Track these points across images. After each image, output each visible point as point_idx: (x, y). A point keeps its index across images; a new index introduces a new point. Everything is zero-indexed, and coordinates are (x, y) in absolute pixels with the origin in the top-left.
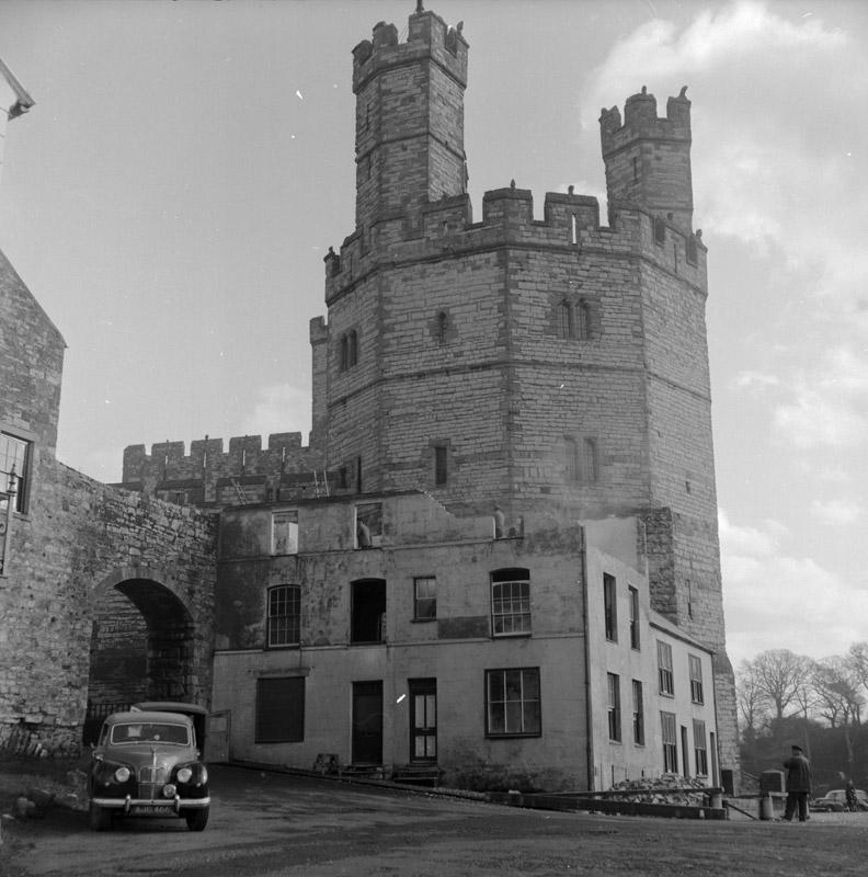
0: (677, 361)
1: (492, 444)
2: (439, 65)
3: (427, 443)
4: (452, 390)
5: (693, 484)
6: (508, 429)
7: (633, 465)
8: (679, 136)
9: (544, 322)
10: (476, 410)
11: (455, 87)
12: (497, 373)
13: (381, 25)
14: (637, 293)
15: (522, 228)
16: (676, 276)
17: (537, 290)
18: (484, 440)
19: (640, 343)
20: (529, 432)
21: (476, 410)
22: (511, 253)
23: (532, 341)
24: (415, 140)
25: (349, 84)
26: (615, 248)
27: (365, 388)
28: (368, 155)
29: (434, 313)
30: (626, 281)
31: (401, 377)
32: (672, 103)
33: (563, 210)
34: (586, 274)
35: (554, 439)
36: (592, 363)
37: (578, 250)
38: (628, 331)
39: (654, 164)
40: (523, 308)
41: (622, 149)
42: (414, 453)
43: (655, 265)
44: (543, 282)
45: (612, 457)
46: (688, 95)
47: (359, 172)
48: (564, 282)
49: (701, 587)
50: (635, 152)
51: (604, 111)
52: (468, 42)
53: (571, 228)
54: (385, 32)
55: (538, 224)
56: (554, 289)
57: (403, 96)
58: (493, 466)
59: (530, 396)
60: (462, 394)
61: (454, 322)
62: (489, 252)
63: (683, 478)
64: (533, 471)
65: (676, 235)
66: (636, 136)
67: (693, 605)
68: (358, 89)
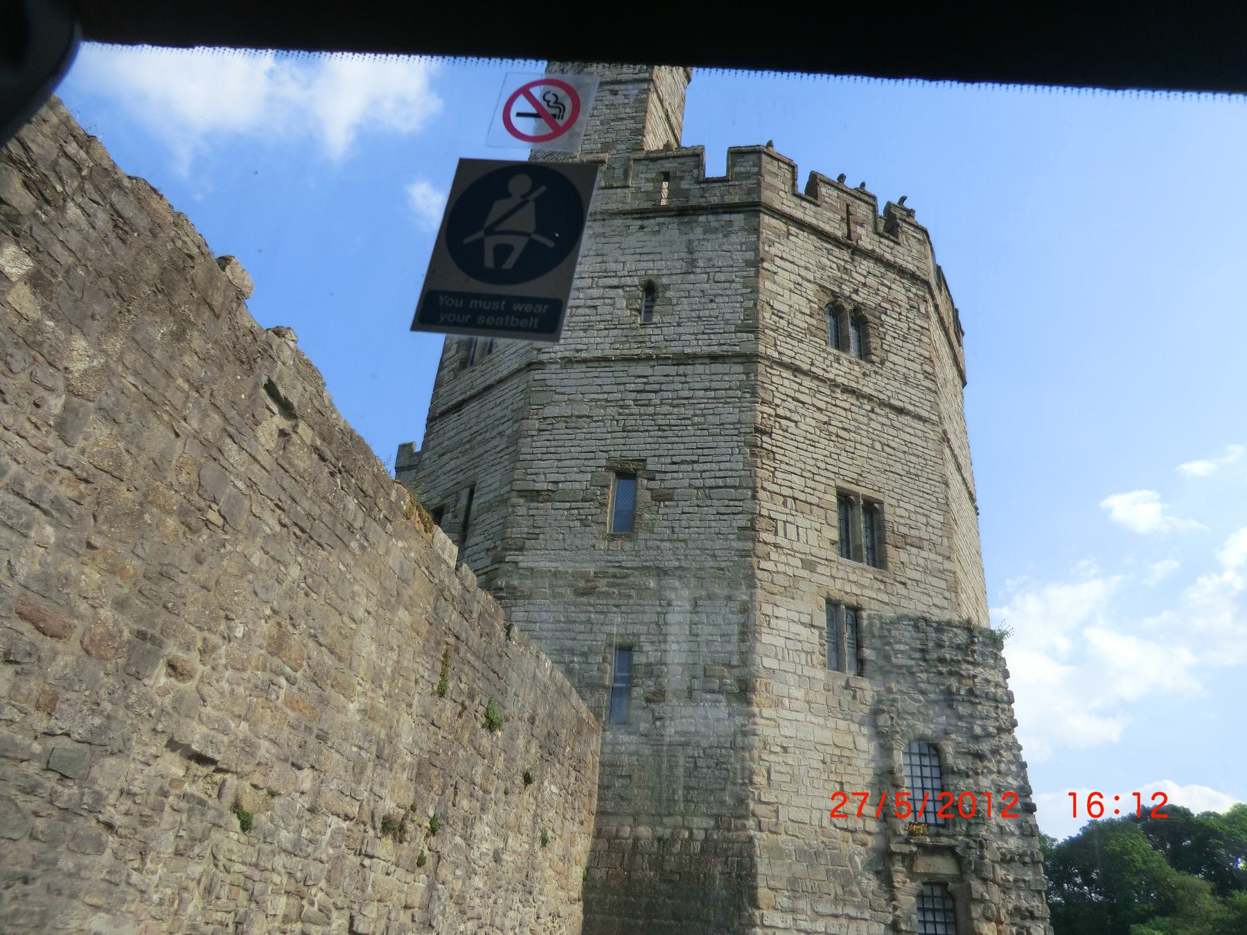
1: (722, 474)
3: (604, 463)
4: (656, 387)
9: (808, 319)
10: (696, 419)
12: (739, 368)
15: (782, 194)
18: (706, 467)
20: (784, 466)
21: (696, 419)
23: (793, 338)
27: (501, 381)
30: (912, 307)
42: (579, 477)
44: (806, 268)
45: (904, 536)
56: (822, 282)
58: (723, 510)
59: (788, 414)
62: (731, 213)
64: (791, 530)
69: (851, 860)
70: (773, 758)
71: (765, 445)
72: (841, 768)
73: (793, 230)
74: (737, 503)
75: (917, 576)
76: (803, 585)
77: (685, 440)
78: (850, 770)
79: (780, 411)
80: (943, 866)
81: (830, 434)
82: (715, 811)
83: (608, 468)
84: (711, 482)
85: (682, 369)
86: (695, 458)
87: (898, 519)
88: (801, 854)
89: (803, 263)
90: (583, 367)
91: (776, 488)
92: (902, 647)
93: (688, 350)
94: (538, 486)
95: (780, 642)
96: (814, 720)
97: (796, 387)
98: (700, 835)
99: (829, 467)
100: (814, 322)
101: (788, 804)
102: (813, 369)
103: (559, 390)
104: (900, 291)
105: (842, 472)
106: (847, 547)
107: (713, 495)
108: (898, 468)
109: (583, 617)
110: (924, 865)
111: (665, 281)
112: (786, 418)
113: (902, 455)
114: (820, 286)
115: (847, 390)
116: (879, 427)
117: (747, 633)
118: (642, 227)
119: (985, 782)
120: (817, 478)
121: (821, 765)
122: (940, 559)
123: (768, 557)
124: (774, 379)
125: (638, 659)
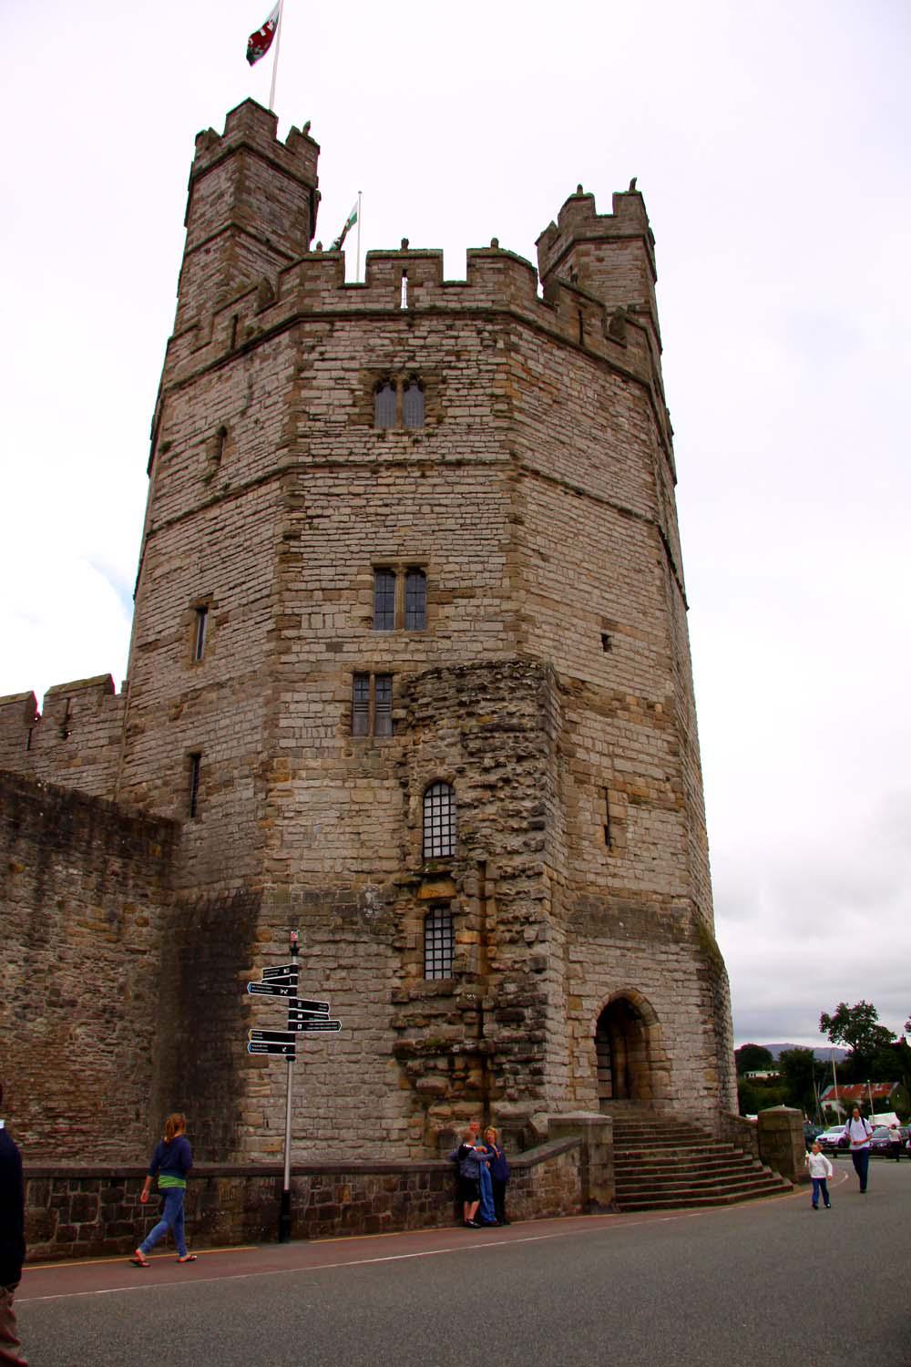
0: (586, 462)
3: (187, 605)
5: (616, 638)
6: (282, 561)
7: (486, 601)
8: (628, 229)
9: (348, 410)
12: (276, 485)
13: (198, 136)
14: (504, 360)
15: (324, 294)
16: (579, 348)
17: (343, 369)
18: (249, 585)
19: (505, 424)
20: (311, 563)
22: (308, 327)
24: (219, 239)
26: (467, 304)
29: (213, 431)
31: (170, 524)
33: (389, 266)
34: (421, 342)
35: (354, 570)
36: (423, 457)
37: (413, 316)
38: (486, 411)
39: (594, 265)
40: (317, 393)
42: (173, 623)
43: (538, 330)
44: (353, 358)
46: (638, 188)
48: (386, 355)
49: (636, 800)
50: (571, 260)
52: (318, 141)
53: (398, 288)
57: (210, 199)
58: (259, 619)
59: (319, 512)
60: (233, 527)
61: (233, 435)
62: (280, 334)
63: (597, 628)
65: (582, 300)
66: (571, 239)
67: (614, 830)
69: (363, 896)
70: (286, 822)
71: (293, 550)
72: (357, 820)
73: (338, 325)
74: (268, 610)
75: (466, 625)
76: (327, 668)
77: (238, 565)
78: (369, 821)
79: (310, 512)
80: (442, 889)
81: (368, 515)
82: (243, 873)
83: (190, 608)
84: (252, 598)
85: (239, 502)
86: (242, 580)
87: (443, 576)
88: (311, 896)
89: (347, 355)
90: (178, 526)
91: (303, 586)
92: (425, 700)
93: (243, 482)
94: (150, 639)
95: (300, 723)
96: (332, 784)
97: (330, 482)
98: (233, 892)
99: (363, 548)
100: (357, 410)
101: (301, 858)
102: (351, 458)
103: (164, 551)
104: (468, 337)
105: (379, 548)
106: (381, 616)
107: (253, 609)
108: (450, 523)
109: (172, 738)
110: (427, 891)
111: (233, 422)
112: (318, 516)
113: (457, 510)
114: (369, 369)
115: (391, 465)
116: (429, 489)
117: (271, 723)
118: (220, 377)
119: (491, 810)
120: (348, 563)
121: (335, 821)
122: (497, 602)
123: (287, 651)
124: (306, 484)
125: (203, 762)
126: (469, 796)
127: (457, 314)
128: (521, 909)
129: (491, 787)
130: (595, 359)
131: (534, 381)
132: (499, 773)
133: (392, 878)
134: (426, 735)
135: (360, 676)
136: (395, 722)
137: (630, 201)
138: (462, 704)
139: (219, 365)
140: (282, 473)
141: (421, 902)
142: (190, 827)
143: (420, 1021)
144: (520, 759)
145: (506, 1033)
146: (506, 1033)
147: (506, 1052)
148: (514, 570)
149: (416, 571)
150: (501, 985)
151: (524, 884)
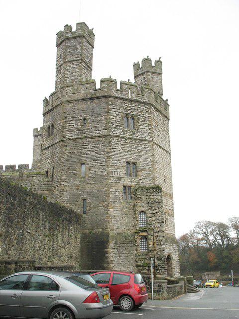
2: (86, 39)
11: (90, 47)
13: (67, 26)
25: (55, 44)
28: (60, 66)
32: (156, 62)
39: (151, 79)
41: (140, 75)
43: (155, 108)
46: (161, 60)
47: (57, 71)
49: (169, 215)
51: (134, 63)
54: (68, 27)
55: (118, 90)
66: (146, 70)
68: (58, 46)
73: (116, 100)
80: (145, 234)
104: (143, 108)
106: (129, 174)
110: (141, 234)
119: (154, 218)
126: (150, 215)
127: (141, 102)
128: (160, 238)
129: (154, 214)
130: (162, 114)
131: (155, 120)
132: (157, 211)
133: (133, 231)
134: (139, 201)
135: (125, 187)
136: (132, 197)
137: (159, 62)
138: (147, 196)
139: (82, 100)
140: (105, 136)
141: (140, 236)
142: (84, 216)
143: (141, 260)
144: (159, 208)
145: (159, 262)
146: (159, 262)
147: (160, 266)
148: (153, 165)
149: (134, 164)
150: (157, 253)
151: (160, 233)
